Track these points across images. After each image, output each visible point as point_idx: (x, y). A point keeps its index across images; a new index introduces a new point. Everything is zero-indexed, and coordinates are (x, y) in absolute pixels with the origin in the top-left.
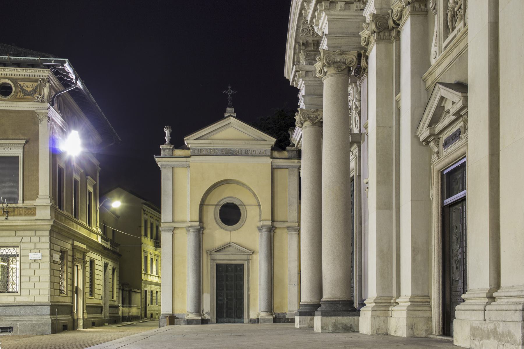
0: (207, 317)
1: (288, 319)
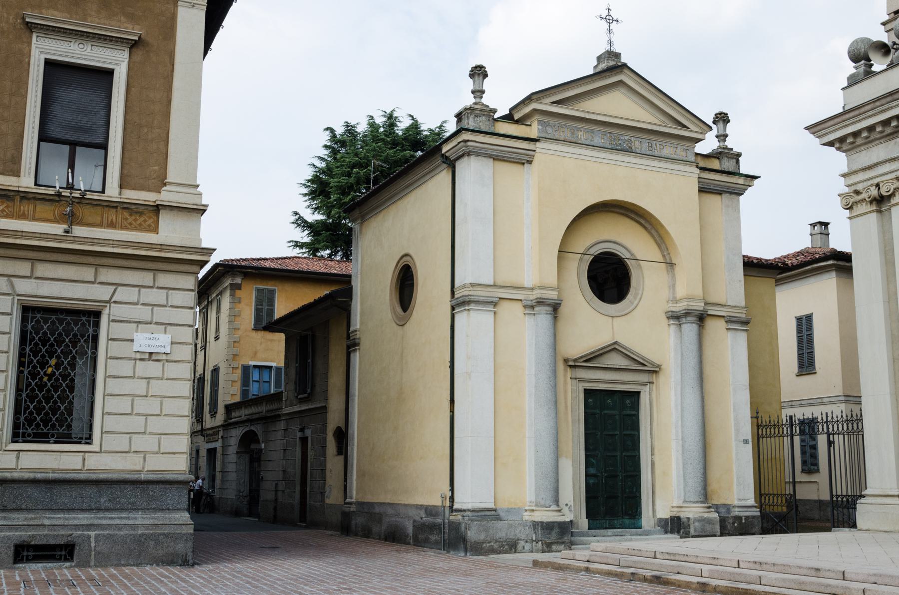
1: (740, 518)
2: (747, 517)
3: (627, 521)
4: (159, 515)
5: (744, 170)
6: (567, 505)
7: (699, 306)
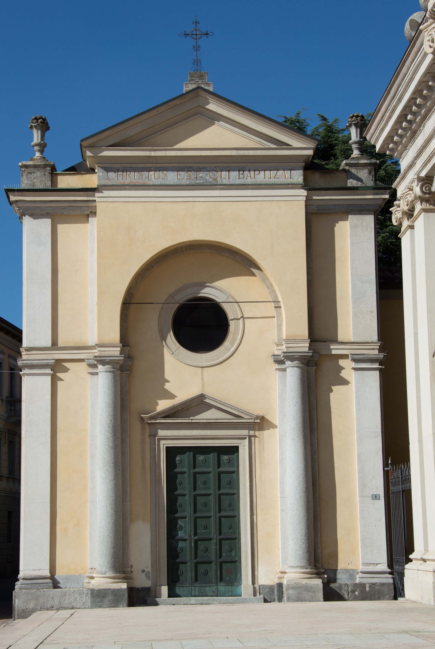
1: (363, 585)
2: (372, 585)
3: (222, 588)
6: (143, 571)
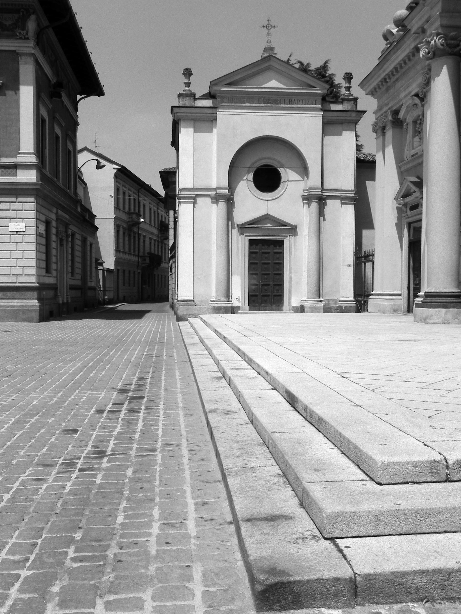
0: (236, 304)
1: (341, 307)
4: (25, 301)
5: (359, 109)
7: (319, 192)
